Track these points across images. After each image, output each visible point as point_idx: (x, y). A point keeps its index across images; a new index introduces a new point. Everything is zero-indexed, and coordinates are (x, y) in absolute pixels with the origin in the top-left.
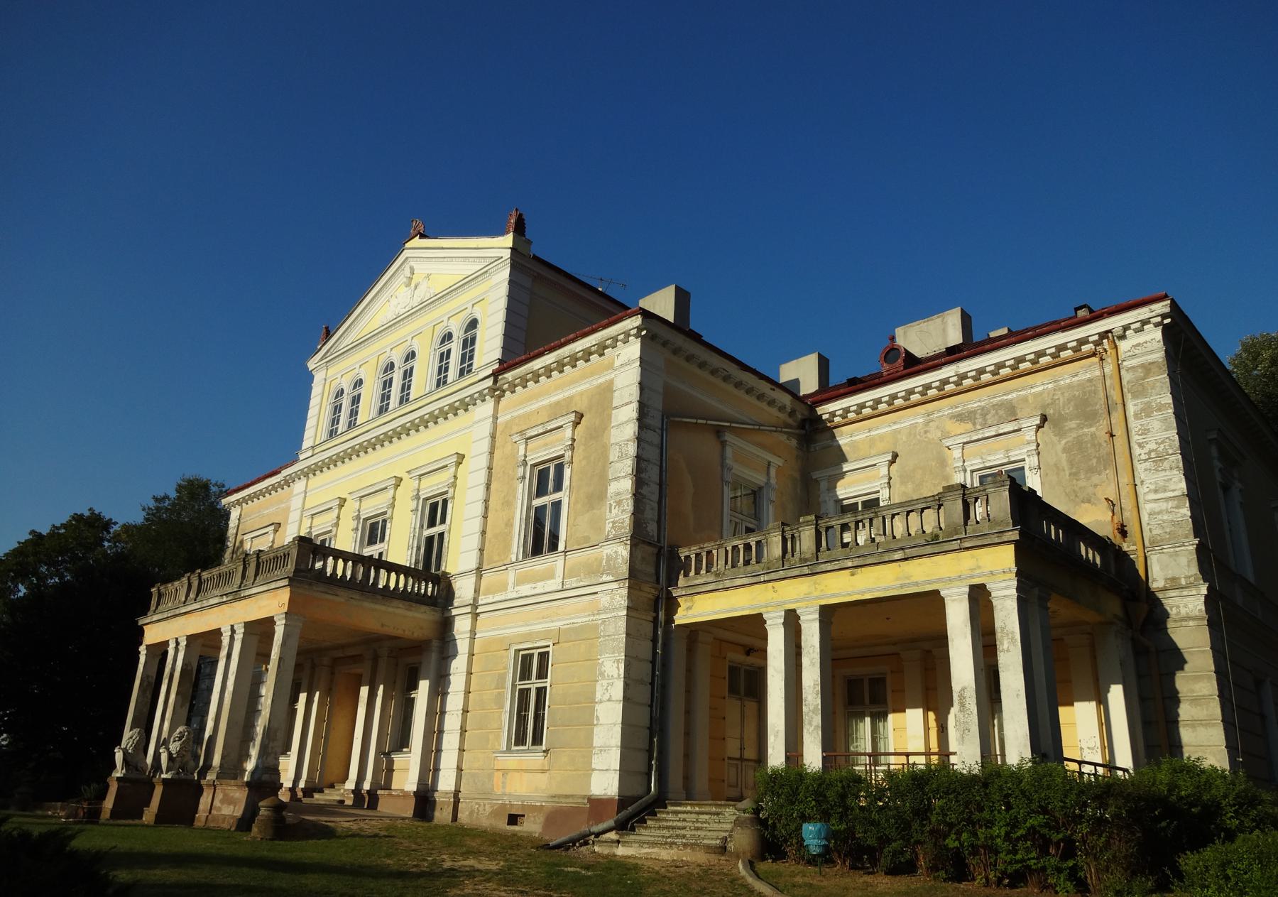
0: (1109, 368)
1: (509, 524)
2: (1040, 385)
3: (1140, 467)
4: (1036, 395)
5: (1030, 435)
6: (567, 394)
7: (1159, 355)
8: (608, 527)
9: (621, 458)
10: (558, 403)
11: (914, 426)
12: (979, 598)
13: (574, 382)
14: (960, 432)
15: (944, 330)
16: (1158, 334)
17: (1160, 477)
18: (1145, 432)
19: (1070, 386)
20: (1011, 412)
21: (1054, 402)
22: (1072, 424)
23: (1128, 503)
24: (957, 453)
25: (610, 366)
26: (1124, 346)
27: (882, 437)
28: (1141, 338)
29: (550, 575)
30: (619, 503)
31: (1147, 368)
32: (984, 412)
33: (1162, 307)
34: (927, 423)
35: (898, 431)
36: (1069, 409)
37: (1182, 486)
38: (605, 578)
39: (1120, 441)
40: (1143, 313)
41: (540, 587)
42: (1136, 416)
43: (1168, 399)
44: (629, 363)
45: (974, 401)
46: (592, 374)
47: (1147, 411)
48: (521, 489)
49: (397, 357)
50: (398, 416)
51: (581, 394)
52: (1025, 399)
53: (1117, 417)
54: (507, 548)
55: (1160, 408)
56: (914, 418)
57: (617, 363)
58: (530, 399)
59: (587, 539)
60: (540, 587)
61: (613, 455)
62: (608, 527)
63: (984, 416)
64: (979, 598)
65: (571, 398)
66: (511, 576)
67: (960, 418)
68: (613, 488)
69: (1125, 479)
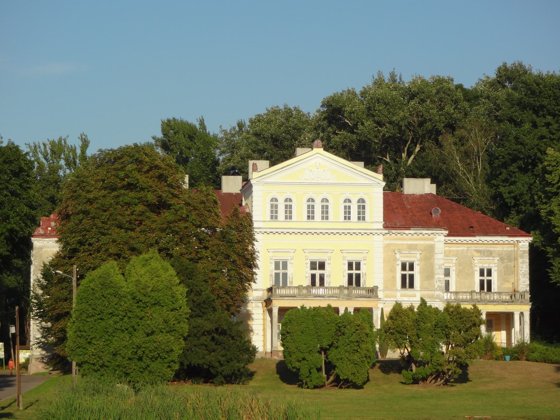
0: (516, 249)
1: (394, 278)
2: (499, 248)
3: (520, 276)
4: (498, 251)
5: (496, 261)
7: (527, 249)
8: (436, 287)
9: (439, 268)
11: (463, 250)
12: (522, 314)
13: (417, 240)
15: (424, 186)
16: (528, 244)
17: (524, 279)
18: (522, 268)
19: (506, 251)
22: (506, 261)
23: (516, 284)
25: (432, 239)
26: (520, 244)
27: (453, 251)
28: (524, 244)
29: (415, 296)
30: (440, 281)
31: (524, 252)
32: (484, 252)
33: (530, 239)
34: (467, 250)
35: (459, 250)
37: (528, 282)
38: (436, 300)
39: (516, 268)
40: (527, 238)
42: (521, 263)
43: (528, 261)
44: (440, 241)
45: (482, 248)
46: (425, 240)
47: (523, 262)
48: (399, 268)
50: (318, 223)
51: (421, 244)
52: (495, 251)
53: (516, 262)
55: (526, 263)
57: (436, 240)
58: (398, 239)
59: (428, 288)
61: (436, 267)
62: (436, 287)
63: (484, 252)
64: (522, 314)
65: (417, 245)
66: (398, 294)
67: (477, 251)
68: (437, 276)
69: (516, 278)
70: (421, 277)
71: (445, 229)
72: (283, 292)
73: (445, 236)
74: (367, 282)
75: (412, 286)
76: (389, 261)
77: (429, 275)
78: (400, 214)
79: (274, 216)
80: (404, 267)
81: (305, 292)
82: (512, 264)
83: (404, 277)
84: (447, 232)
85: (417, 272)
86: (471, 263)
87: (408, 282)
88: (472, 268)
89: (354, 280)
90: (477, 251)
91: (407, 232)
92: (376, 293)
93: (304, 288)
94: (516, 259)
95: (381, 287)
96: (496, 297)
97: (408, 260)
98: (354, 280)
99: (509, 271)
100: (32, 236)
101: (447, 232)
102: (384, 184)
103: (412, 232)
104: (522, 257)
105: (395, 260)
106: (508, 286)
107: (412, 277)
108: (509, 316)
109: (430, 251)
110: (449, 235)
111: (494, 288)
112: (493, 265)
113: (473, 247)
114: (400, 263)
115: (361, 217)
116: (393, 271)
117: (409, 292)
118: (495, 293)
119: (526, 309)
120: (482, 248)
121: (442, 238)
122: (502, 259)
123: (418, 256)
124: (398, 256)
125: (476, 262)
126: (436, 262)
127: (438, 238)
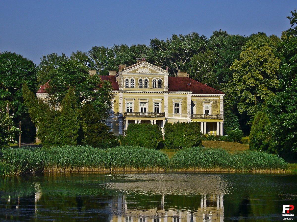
1: (172, 109)
2: (212, 98)
5: (211, 103)
6: (181, 96)
10: (178, 97)
14: (204, 100)
20: (209, 100)
21: (213, 100)
24: (204, 103)
25: (186, 95)
35: (197, 99)
36: (215, 101)
41: (178, 117)
46: (184, 95)
48: (174, 106)
49: (143, 80)
54: (172, 112)
56: (199, 98)
57: (187, 95)
60: (178, 117)
61: (188, 105)
62: (188, 113)
66: (173, 115)
67: (204, 99)
68: (188, 109)
70: (182, 109)
71: (191, 91)
72: (130, 114)
73: (191, 94)
74: (161, 111)
75: (179, 112)
76: (170, 102)
77: (185, 108)
78: (175, 85)
79: (127, 87)
80: (175, 105)
81: (138, 114)
82: (217, 104)
83: (175, 109)
84: (192, 92)
85: (180, 107)
86: (202, 104)
87: (177, 111)
88: (202, 105)
89: (157, 110)
90: (204, 99)
91: (177, 92)
92: (165, 115)
93: (138, 113)
94: (219, 102)
95: (166, 113)
96: (210, 116)
97: (177, 102)
98: (157, 110)
99: (215, 106)
100: (37, 93)
101: (192, 92)
102: (168, 74)
103: (179, 92)
104: (221, 102)
105: (172, 102)
106: (215, 112)
107: (179, 109)
108: (216, 123)
109: (186, 99)
110: (192, 93)
111: (210, 113)
112: (210, 105)
113: (203, 98)
114: (174, 104)
115: (160, 87)
116: (171, 107)
117: (178, 114)
118: (211, 115)
119: (222, 122)
120: (206, 98)
121: (190, 95)
122: (213, 102)
123: (181, 101)
124: (173, 101)
125: (204, 103)
126: (188, 103)
127: (189, 95)
